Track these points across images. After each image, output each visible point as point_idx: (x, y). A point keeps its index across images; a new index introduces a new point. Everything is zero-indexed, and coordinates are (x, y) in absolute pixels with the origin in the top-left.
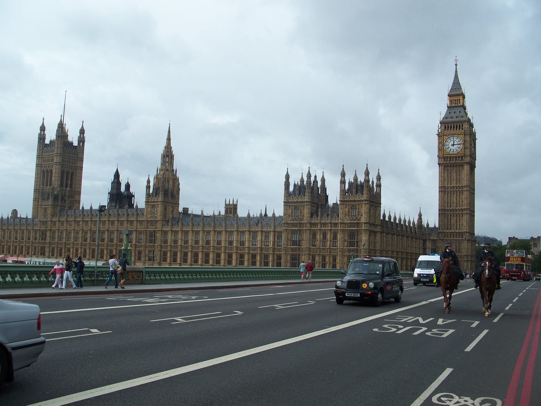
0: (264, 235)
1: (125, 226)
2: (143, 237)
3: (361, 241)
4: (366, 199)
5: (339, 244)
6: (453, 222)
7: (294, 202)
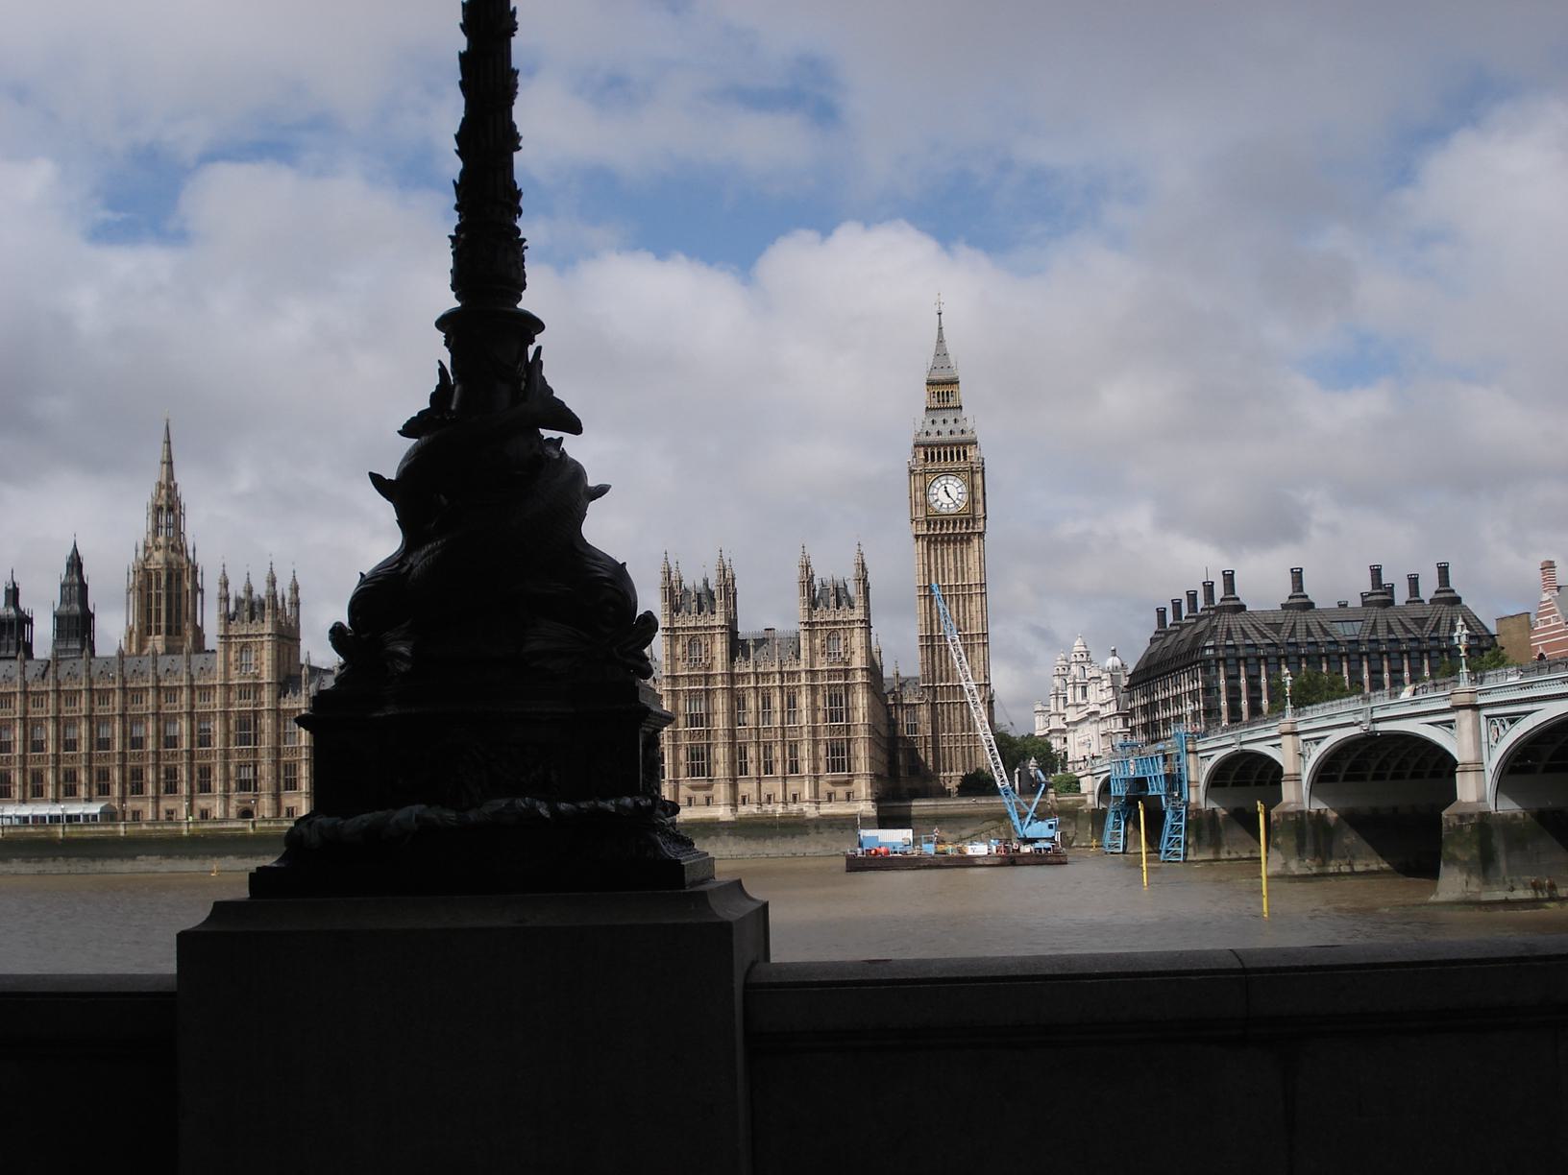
2: (217, 727)
5: (804, 718)
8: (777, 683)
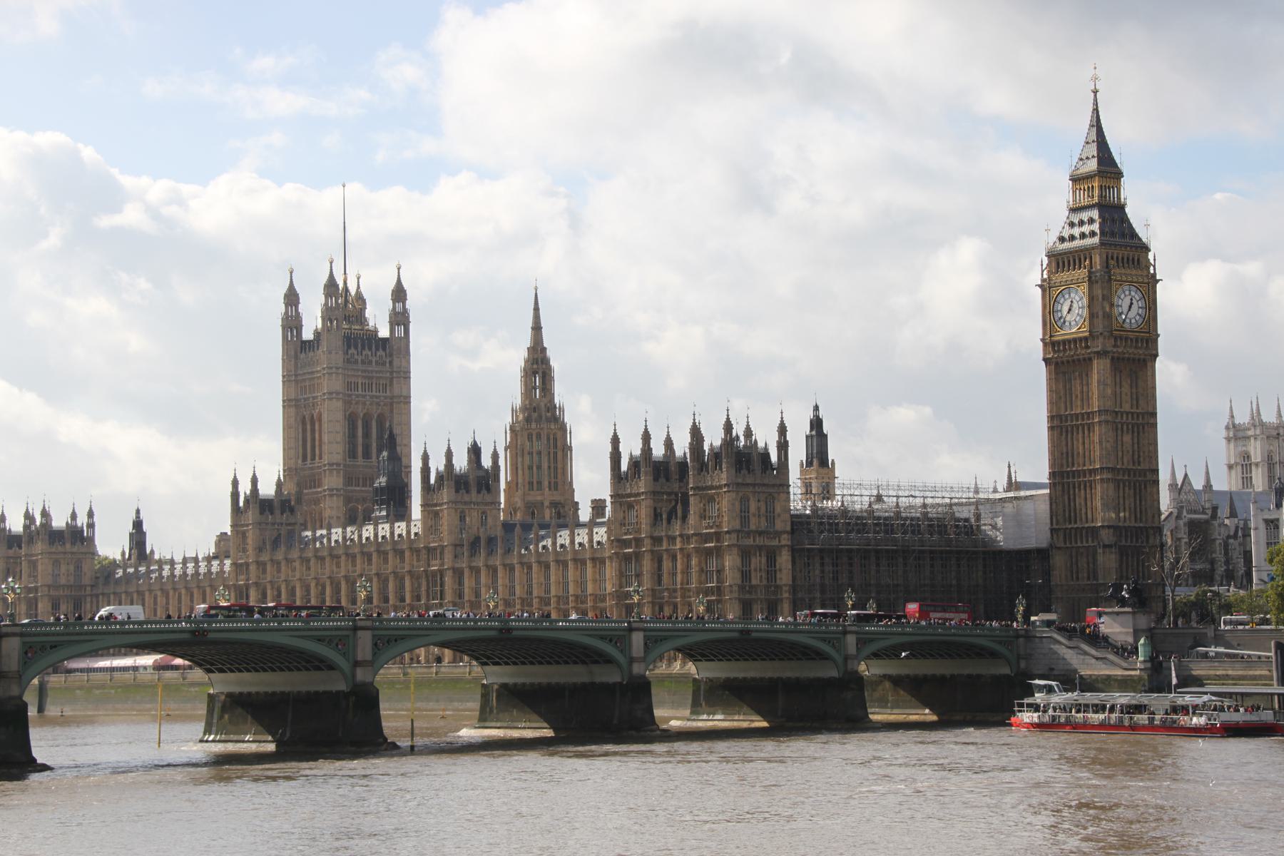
1: (328, 568)
6: (1080, 504)
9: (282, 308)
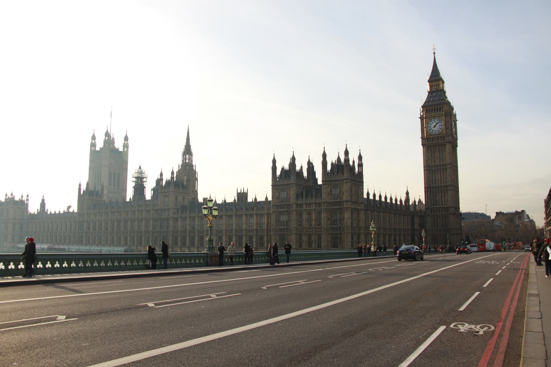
0: (259, 217)
3: (344, 220)
4: (346, 178)
7: (281, 185)
8: (314, 208)
9: (90, 141)
